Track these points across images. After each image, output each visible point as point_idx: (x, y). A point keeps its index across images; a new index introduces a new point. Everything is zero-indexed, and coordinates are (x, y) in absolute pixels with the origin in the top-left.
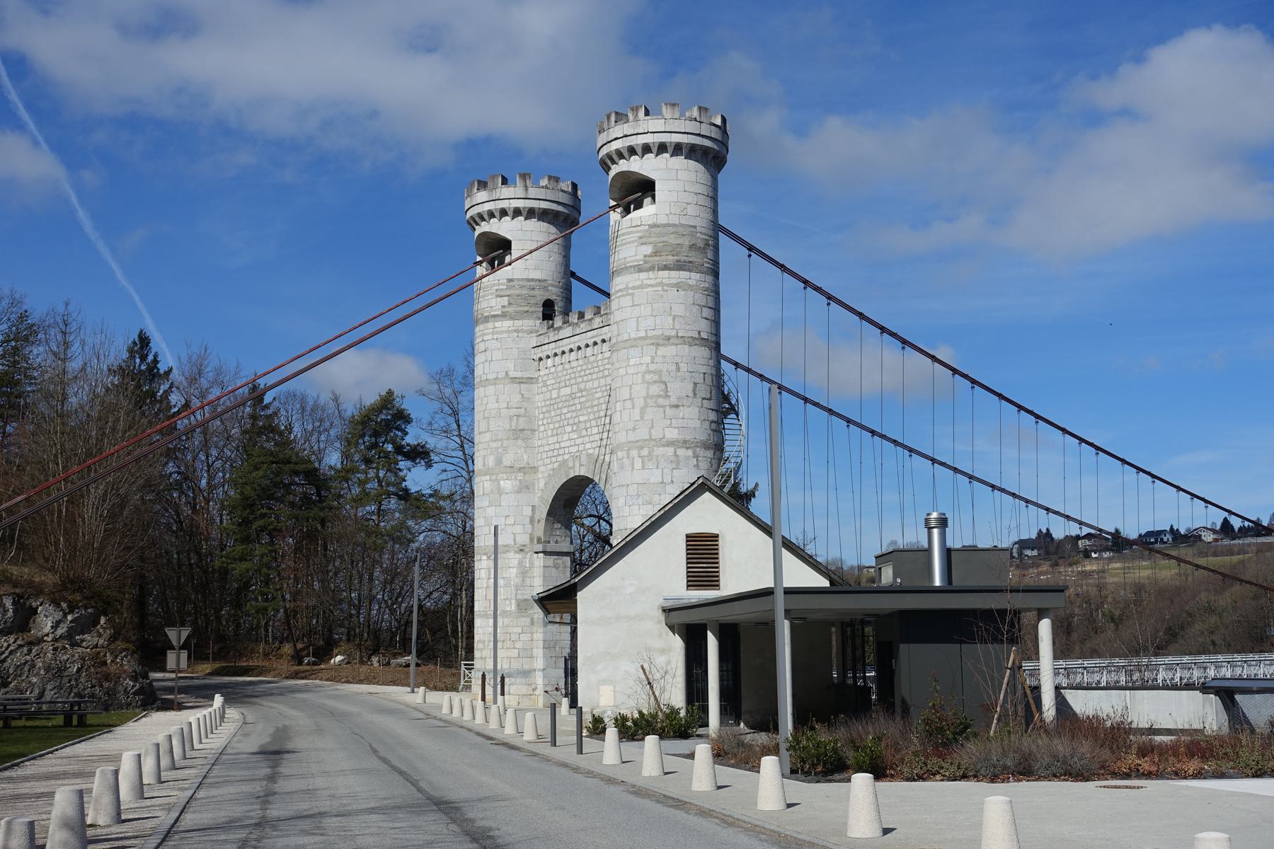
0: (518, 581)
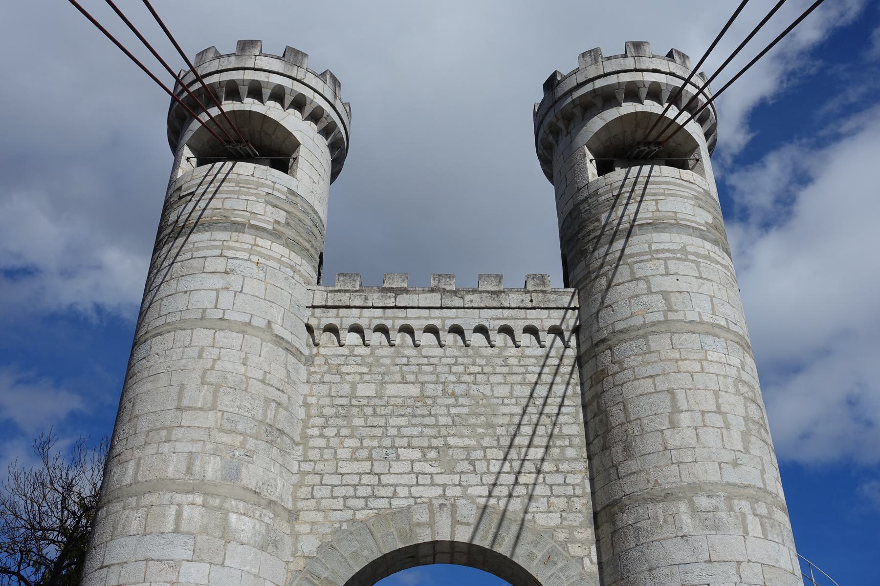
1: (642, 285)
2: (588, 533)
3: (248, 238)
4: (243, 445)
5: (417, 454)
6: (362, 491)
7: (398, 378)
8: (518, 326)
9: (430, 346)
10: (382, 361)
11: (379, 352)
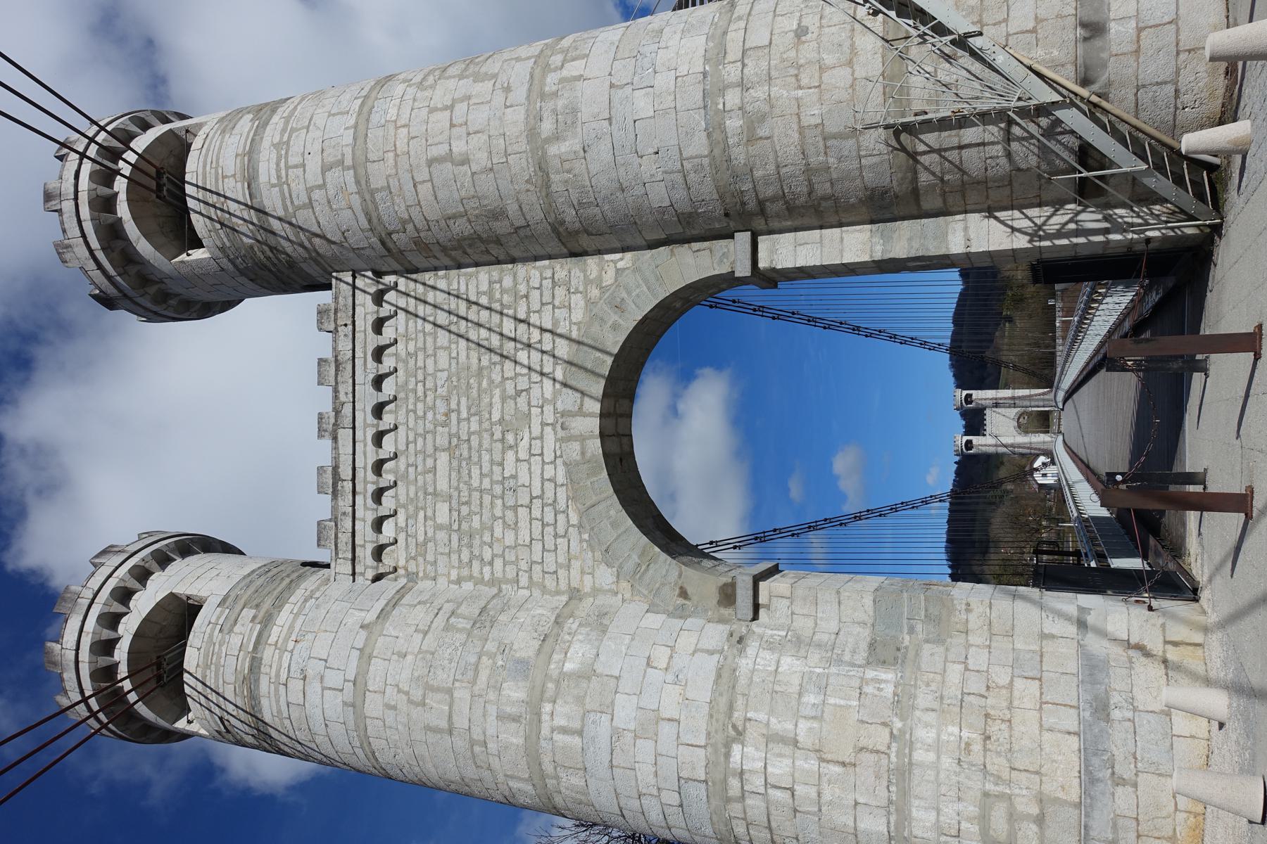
0: (815, 656)
1: (317, 195)
2: (592, 262)
3: (268, 654)
4: (492, 656)
5: (510, 455)
6: (549, 518)
7: (429, 477)
8: (373, 341)
9: (396, 441)
10: (412, 495)
11: (403, 499)
